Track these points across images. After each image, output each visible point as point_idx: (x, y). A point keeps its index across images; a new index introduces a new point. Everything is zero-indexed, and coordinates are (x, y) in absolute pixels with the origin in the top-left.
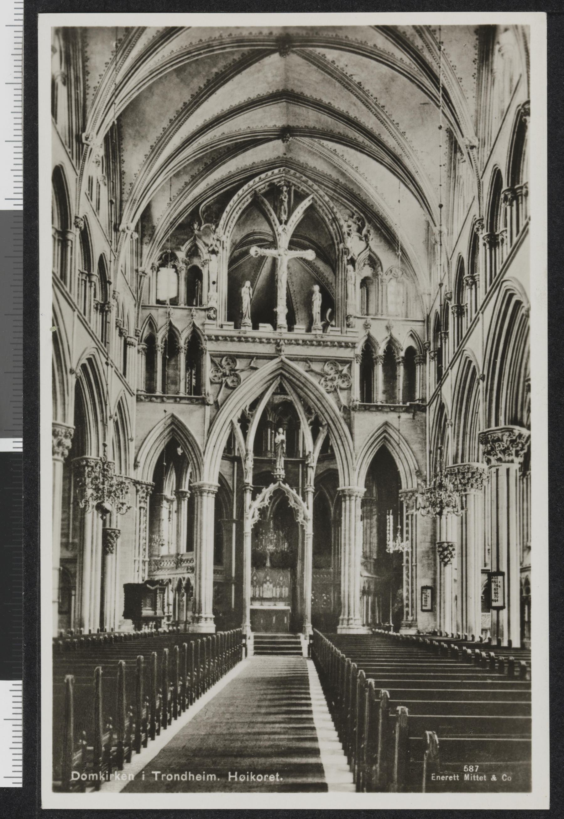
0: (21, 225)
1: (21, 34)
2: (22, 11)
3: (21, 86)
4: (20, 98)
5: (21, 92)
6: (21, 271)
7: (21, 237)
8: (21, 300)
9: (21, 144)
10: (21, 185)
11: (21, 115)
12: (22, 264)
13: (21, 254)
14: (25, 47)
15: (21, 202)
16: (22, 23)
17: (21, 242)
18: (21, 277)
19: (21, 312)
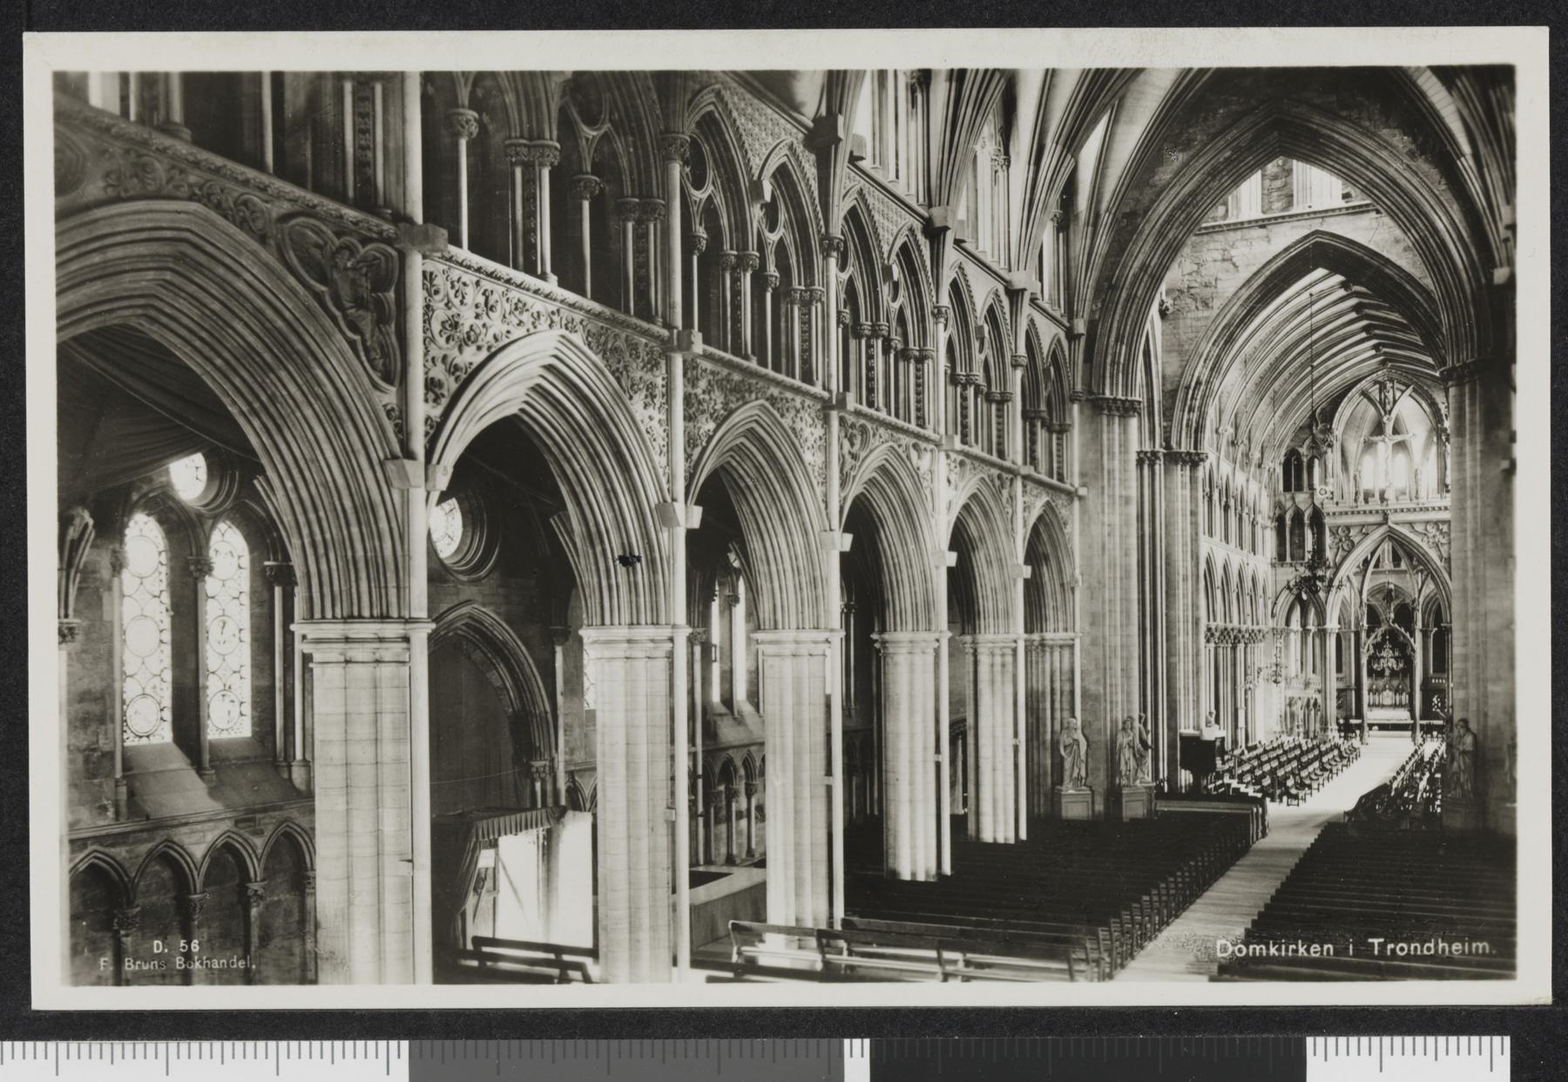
0: (438, 1043)
1: (74, 1045)
2: (29, 1044)
3: (173, 1045)
4: (195, 1045)
5: (184, 1045)
6: (526, 1043)
7: (460, 1043)
8: (581, 1042)
9: (283, 1044)
10: (360, 1043)
11: (228, 1044)
12: (512, 1041)
13: (493, 1043)
14: (96, 1039)
15: (393, 1043)
16: (52, 1045)
17: (471, 1043)
18: (537, 1043)
19: (603, 1042)
